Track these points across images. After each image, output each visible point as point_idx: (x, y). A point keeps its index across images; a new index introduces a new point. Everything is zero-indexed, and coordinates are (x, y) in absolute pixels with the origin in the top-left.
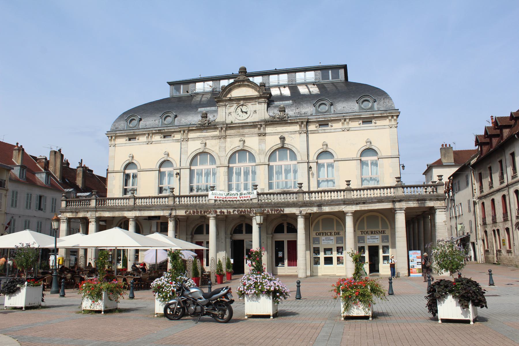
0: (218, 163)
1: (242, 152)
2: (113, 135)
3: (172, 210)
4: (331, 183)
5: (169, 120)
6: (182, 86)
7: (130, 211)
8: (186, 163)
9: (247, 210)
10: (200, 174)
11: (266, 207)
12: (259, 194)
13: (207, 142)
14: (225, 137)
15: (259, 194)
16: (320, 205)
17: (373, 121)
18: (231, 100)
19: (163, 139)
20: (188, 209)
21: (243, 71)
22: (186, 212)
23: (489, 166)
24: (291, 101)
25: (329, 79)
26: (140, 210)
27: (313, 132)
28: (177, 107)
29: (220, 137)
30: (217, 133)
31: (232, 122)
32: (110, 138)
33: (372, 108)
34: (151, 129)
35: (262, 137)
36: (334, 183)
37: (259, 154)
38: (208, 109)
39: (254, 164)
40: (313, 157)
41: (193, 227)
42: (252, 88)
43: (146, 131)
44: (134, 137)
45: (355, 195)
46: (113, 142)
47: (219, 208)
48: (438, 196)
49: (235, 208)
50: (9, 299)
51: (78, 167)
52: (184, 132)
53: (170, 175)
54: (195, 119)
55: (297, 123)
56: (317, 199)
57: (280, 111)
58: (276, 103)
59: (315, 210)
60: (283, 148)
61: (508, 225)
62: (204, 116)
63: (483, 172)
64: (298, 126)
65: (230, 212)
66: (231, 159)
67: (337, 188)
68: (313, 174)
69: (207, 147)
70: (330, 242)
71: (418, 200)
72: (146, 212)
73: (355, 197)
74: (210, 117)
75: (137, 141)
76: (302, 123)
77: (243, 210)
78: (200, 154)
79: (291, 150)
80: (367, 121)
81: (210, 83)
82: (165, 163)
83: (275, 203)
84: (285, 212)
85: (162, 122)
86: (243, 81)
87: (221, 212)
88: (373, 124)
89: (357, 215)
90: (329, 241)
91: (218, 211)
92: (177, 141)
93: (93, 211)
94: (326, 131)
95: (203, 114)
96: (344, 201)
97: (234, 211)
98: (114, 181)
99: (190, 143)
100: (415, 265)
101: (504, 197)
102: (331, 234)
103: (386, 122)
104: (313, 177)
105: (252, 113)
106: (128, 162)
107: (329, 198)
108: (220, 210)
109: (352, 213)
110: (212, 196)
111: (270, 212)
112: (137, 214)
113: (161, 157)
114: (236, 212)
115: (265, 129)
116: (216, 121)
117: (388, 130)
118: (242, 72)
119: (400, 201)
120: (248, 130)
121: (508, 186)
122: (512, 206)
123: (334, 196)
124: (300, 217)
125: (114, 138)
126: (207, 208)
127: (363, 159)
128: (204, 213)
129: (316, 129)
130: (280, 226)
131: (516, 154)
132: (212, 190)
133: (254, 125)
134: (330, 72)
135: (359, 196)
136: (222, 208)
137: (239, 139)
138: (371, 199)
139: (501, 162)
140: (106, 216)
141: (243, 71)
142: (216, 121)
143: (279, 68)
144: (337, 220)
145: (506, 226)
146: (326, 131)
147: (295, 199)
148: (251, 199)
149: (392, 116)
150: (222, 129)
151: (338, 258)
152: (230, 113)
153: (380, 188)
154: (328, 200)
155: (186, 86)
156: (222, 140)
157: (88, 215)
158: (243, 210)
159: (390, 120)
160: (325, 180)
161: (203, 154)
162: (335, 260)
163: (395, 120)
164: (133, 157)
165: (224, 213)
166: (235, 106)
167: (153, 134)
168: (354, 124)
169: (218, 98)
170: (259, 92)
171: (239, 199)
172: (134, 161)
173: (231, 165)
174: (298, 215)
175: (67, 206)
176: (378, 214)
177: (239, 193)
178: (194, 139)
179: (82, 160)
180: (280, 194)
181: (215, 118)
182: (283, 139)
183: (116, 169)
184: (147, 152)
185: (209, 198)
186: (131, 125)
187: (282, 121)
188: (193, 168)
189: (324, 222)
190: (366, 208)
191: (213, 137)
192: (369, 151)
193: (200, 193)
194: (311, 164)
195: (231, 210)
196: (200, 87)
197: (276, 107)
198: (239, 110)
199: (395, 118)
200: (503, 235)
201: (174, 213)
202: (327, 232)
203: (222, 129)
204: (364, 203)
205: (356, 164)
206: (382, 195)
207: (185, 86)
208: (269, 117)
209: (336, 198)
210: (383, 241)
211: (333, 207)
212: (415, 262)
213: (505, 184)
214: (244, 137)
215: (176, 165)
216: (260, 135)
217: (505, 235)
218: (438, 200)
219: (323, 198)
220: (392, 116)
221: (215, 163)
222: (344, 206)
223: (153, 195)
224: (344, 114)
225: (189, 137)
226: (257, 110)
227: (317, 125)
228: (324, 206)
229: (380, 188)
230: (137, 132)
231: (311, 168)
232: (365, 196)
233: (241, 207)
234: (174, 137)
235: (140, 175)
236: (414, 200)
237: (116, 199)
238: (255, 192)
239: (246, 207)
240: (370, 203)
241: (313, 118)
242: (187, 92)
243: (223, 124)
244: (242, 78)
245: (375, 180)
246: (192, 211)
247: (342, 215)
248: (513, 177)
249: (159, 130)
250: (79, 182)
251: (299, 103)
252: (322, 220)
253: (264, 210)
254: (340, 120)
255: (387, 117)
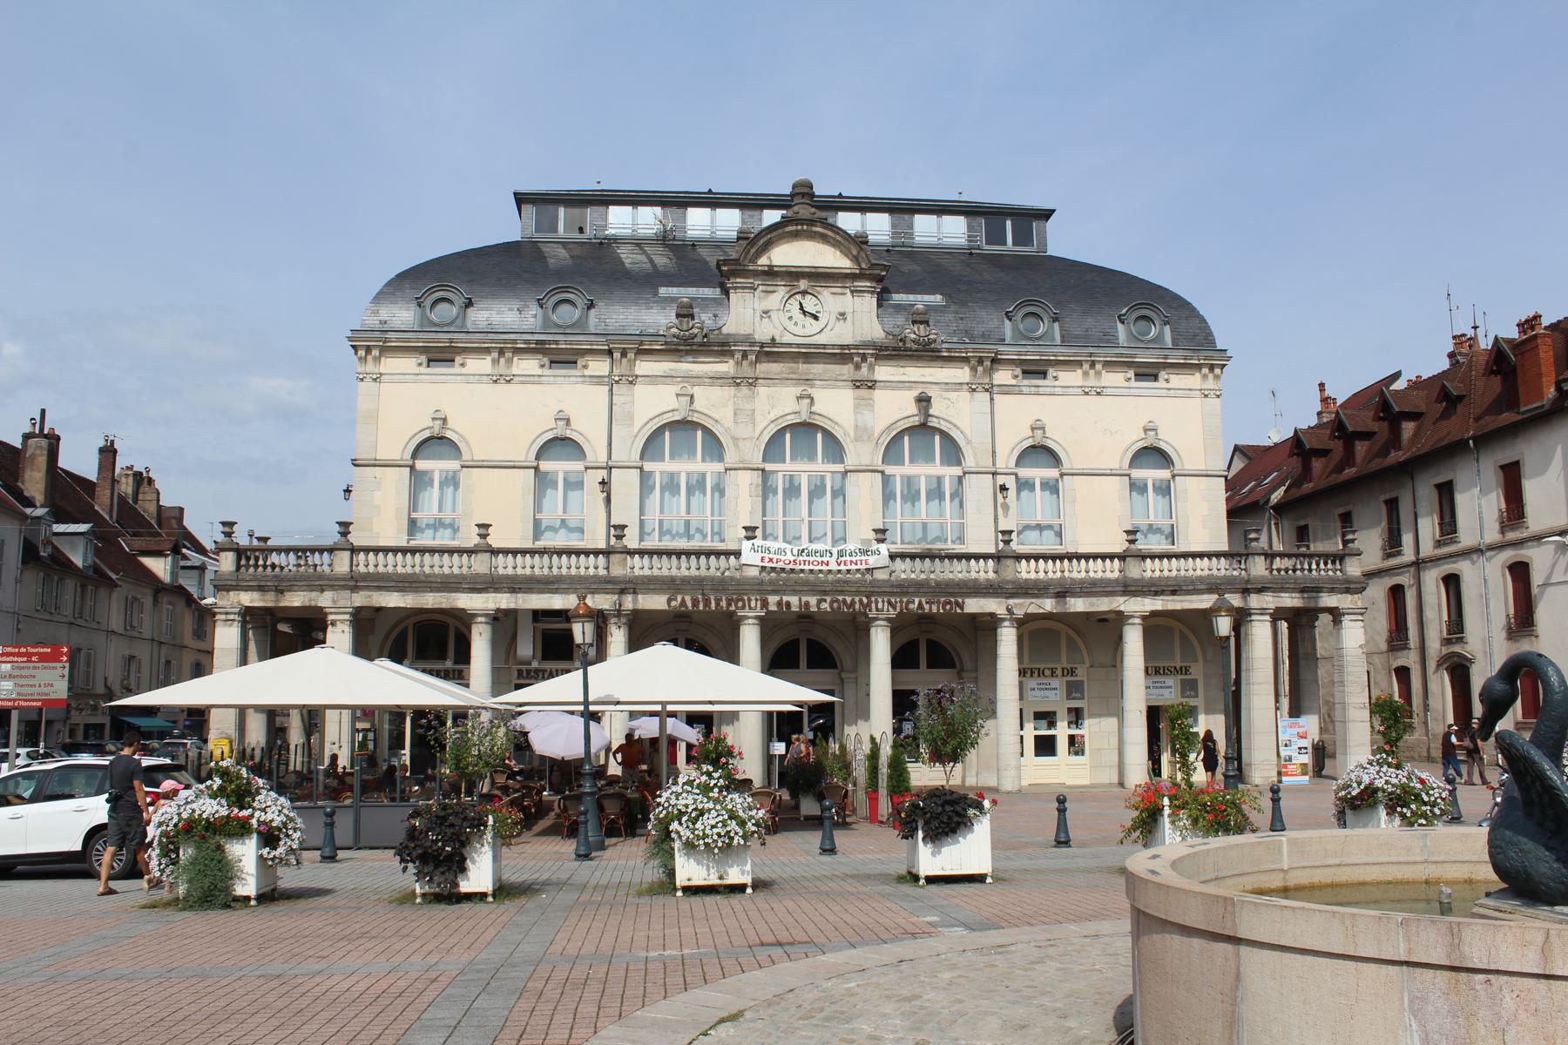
0: (731, 457)
1: (805, 430)
2: (372, 344)
3: (622, 592)
4: (1049, 535)
5: (567, 314)
6: (562, 211)
7: (479, 591)
8: (628, 449)
9: (861, 602)
10: (671, 485)
11: (916, 594)
12: (892, 557)
13: (697, 391)
14: (753, 382)
15: (892, 557)
16: (1063, 591)
17: (1163, 375)
18: (771, 273)
19: (547, 372)
20: (678, 591)
21: (803, 190)
22: (669, 601)
23: (1342, 510)
24: (939, 297)
25: (1005, 244)
26: (513, 590)
27: (1007, 390)
28: (551, 272)
29: (735, 382)
30: (727, 367)
31: (773, 339)
32: (362, 353)
33: (1159, 338)
34: (512, 337)
35: (863, 392)
36: (1059, 534)
37: (857, 439)
38: (692, 291)
39: (840, 468)
40: (1006, 460)
41: (809, 642)
42: (833, 246)
43: (492, 341)
44: (449, 356)
45: (1152, 570)
46: (370, 367)
47: (775, 592)
48: (1348, 581)
49: (825, 593)
50: (933, 854)
51: (26, 437)
52: (624, 354)
53: (574, 484)
54: (659, 319)
55: (966, 360)
56: (1050, 575)
57: (914, 322)
58: (899, 298)
59: (1048, 605)
60: (923, 431)
61: (1410, 659)
62: (685, 311)
63: (1313, 524)
64: (967, 369)
65: (807, 604)
66: (773, 449)
67: (1071, 550)
68: (1006, 507)
69: (697, 405)
70: (1051, 694)
71: (1303, 591)
72: (534, 596)
73: (1148, 574)
74: (705, 318)
75: (457, 369)
76: (980, 361)
77: (849, 600)
78: (673, 426)
79: (945, 436)
80: (1147, 373)
81: (658, 210)
82: (561, 445)
83: (938, 584)
84: (968, 610)
85: (546, 318)
86: (811, 222)
87: (779, 604)
88: (1161, 383)
89: (1025, 624)
90: (1047, 693)
91: (773, 600)
92: (597, 380)
93: (344, 588)
94: (1041, 390)
95: (681, 306)
96: (1125, 586)
97: (820, 602)
98: (377, 494)
99: (640, 389)
100: (1295, 754)
101: (1397, 593)
102: (1053, 674)
103: (1193, 380)
104: (1006, 516)
105: (833, 318)
106: (427, 434)
107: (1083, 575)
108: (777, 598)
109: (1144, 618)
110: (750, 556)
111: (927, 607)
112: (504, 601)
113: (545, 427)
114: (825, 606)
115: (871, 368)
116: (725, 330)
117: (1197, 403)
118: (803, 195)
119: (1260, 591)
120: (821, 366)
121: (1419, 565)
122: (1430, 614)
123: (1097, 570)
124: (1006, 623)
125: (376, 352)
126: (738, 589)
127: (1138, 474)
128: (729, 605)
129: (1014, 382)
130: (942, 645)
131: (1458, 486)
132: (748, 538)
133: (843, 355)
134: (1009, 223)
135: (1157, 574)
136: (784, 592)
137: (798, 390)
138: (1191, 581)
139: (1392, 505)
140: (391, 605)
141: (803, 190)
142: (725, 330)
143: (722, 187)
144: (1069, 639)
145: (1400, 663)
146: (1041, 390)
147: (991, 575)
148: (870, 570)
149: (1212, 368)
150: (745, 355)
151: (1072, 739)
152: (766, 312)
153: (1178, 556)
154: (1082, 581)
155: (576, 211)
156: (744, 390)
157: (325, 600)
158: (849, 600)
159: (1205, 377)
160: (1034, 523)
161: (682, 429)
162: (1062, 745)
163: (1217, 377)
164: (445, 420)
165: (788, 604)
166: (782, 292)
167: (517, 351)
168: (1114, 379)
169: (730, 267)
170: (855, 259)
171: (833, 566)
172: (449, 434)
173: (769, 467)
174: (1003, 620)
175: (238, 567)
176: (1177, 625)
177: (835, 551)
178: (653, 379)
179: (43, 412)
180: (913, 557)
181: (721, 323)
182: (924, 401)
183: (382, 455)
184: (500, 407)
185: (744, 560)
186: (433, 317)
187: (926, 353)
188: (649, 466)
189: (1071, 645)
190: (1178, 607)
191: (716, 379)
192: (1153, 454)
193: (668, 544)
194: (1001, 480)
195: (813, 600)
196: (619, 220)
197: (899, 308)
198: (794, 306)
199: (1217, 371)
200: (1384, 685)
201: (628, 603)
202: (1042, 666)
203: (745, 355)
204: (1174, 593)
205: (1118, 485)
206: (1215, 572)
207: (570, 210)
208: (883, 334)
209: (1099, 575)
210: (1069, 697)
211: (1094, 599)
212: (1295, 747)
213: (1408, 555)
214: (812, 386)
215: (596, 452)
216: (858, 384)
217: (1391, 686)
218: (1348, 591)
219: (1067, 574)
220: (1212, 368)
221: (721, 459)
222: (1122, 599)
223: (329, 542)
224: (1092, 350)
225: (638, 372)
226: (849, 310)
227: (1018, 371)
228: (1074, 595)
229: (1178, 556)
230: (461, 340)
231: (1003, 488)
232: (1174, 573)
233: (842, 592)
234: (585, 367)
235: (470, 478)
236: (1293, 590)
237: (386, 550)
238: (884, 549)
239: (858, 593)
240: (1188, 592)
241: (1009, 352)
242: (581, 230)
243: (753, 344)
244: (805, 211)
245: (1159, 530)
246: (688, 599)
247: (1112, 624)
248: (1438, 544)
249: (537, 342)
250: (34, 483)
251: (964, 304)
252: (1030, 633)
253: (908, 602)
254: (1080, 364)
255: (1198, 367)
